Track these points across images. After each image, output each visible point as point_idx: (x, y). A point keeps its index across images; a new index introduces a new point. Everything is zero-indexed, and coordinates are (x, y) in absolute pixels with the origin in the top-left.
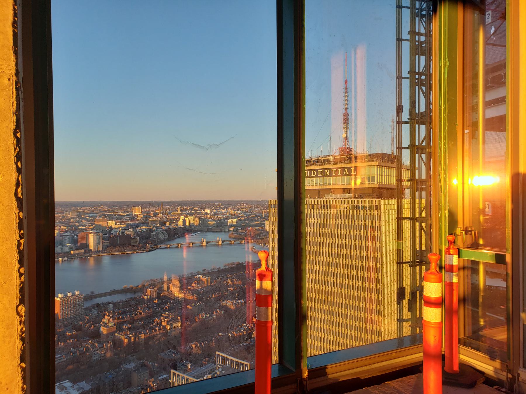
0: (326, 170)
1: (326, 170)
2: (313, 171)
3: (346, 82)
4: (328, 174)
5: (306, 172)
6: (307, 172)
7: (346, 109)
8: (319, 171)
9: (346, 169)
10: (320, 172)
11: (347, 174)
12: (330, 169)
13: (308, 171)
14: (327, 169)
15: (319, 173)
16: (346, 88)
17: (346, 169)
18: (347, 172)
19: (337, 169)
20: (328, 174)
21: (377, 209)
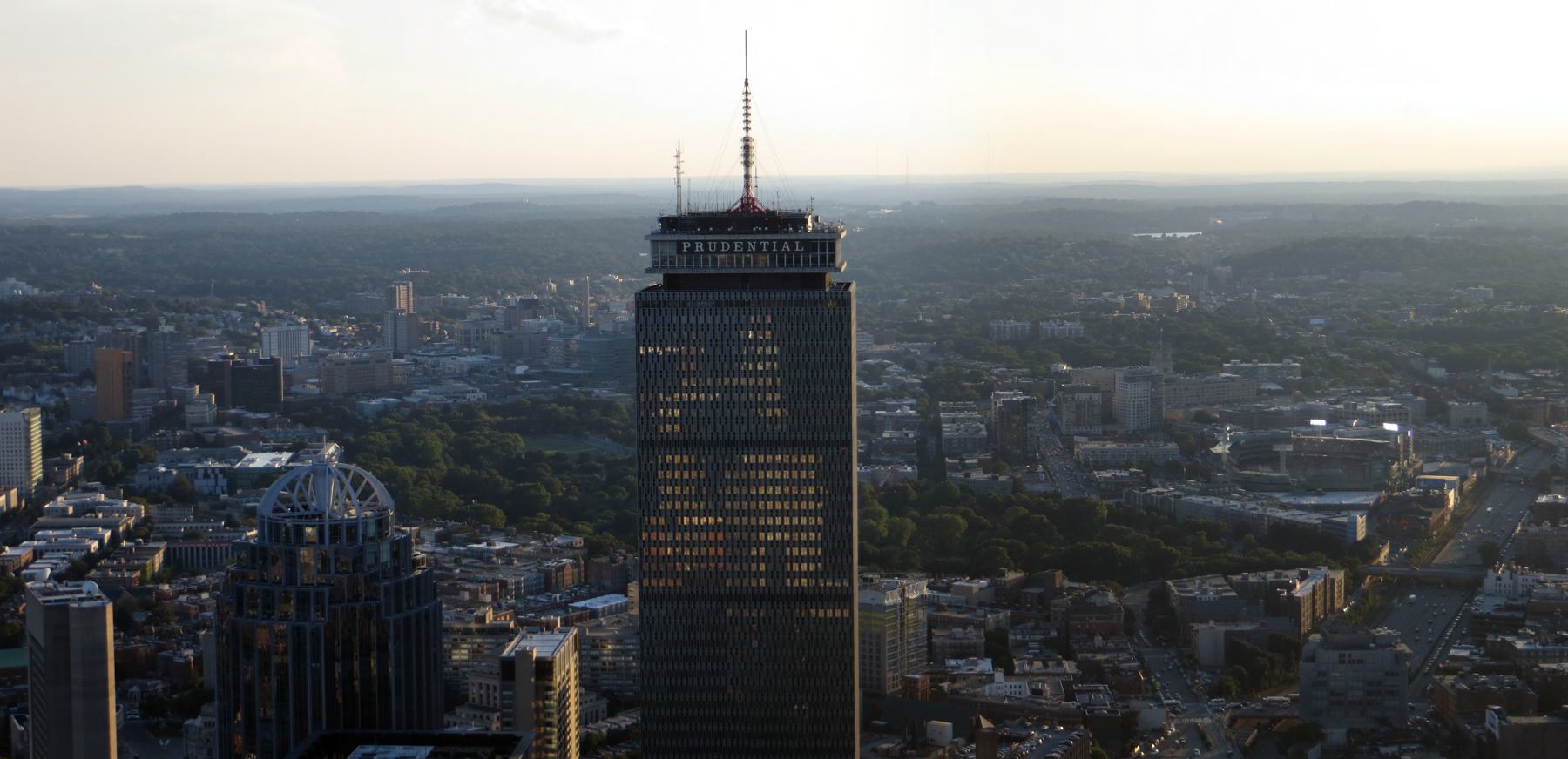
0: (750, 243)
1: (750, 243)
2: (723, 243)
3: (747, 84)
4: (754, 249)
5: (710, 243)
6: (713, 244)
7: (747, 129)
8: (736, 243)
9: (786, 243)
10: (738, 244)
11: (789, 250)
12: (758, 241)
13: (715, 243)
14: (752, 241)
15: (736, 246)
16: (747, 93)
17: (786, 243)
18: (788, 247)
19: (771, 241)
20: (754, 249)
21: (844, 305)
